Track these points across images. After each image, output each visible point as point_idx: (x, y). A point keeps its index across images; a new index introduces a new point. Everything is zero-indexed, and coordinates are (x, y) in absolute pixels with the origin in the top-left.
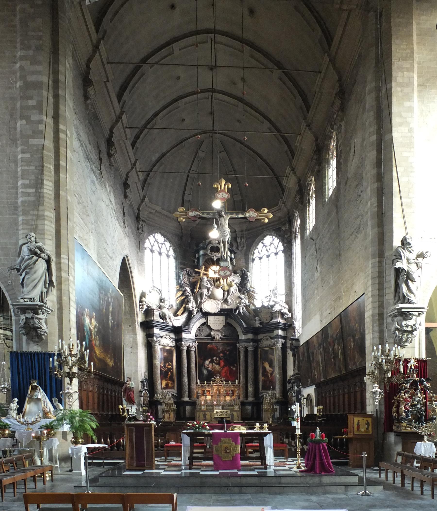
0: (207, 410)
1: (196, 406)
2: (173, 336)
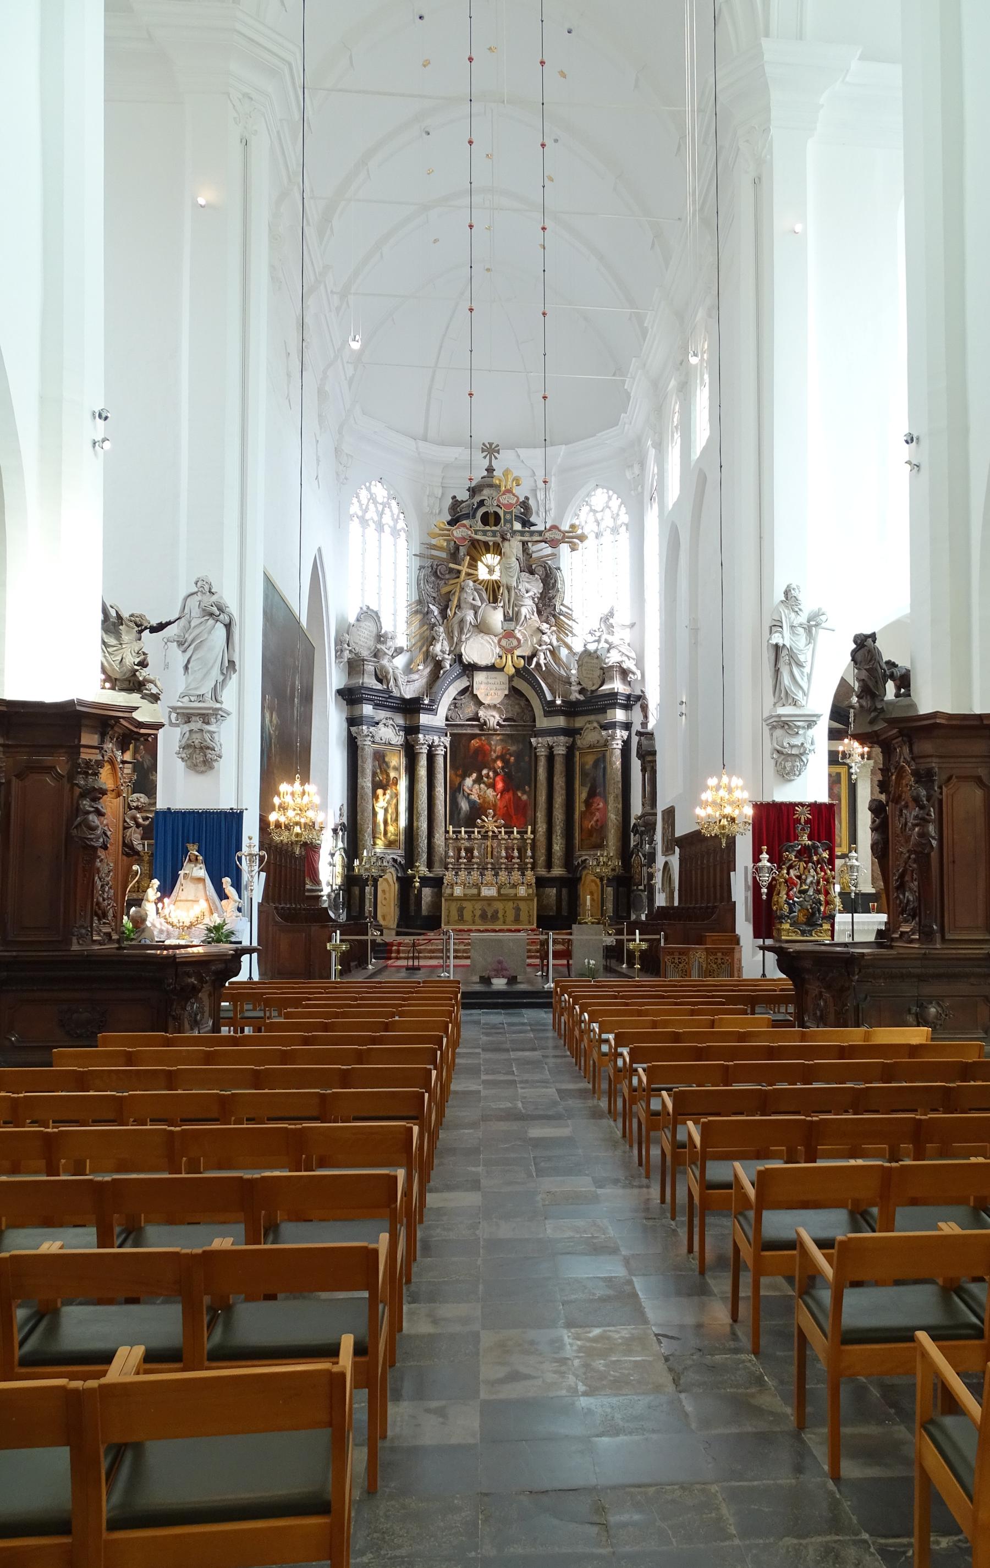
0: (465, 898)
1: (444, 887)
2: (400, 720)
